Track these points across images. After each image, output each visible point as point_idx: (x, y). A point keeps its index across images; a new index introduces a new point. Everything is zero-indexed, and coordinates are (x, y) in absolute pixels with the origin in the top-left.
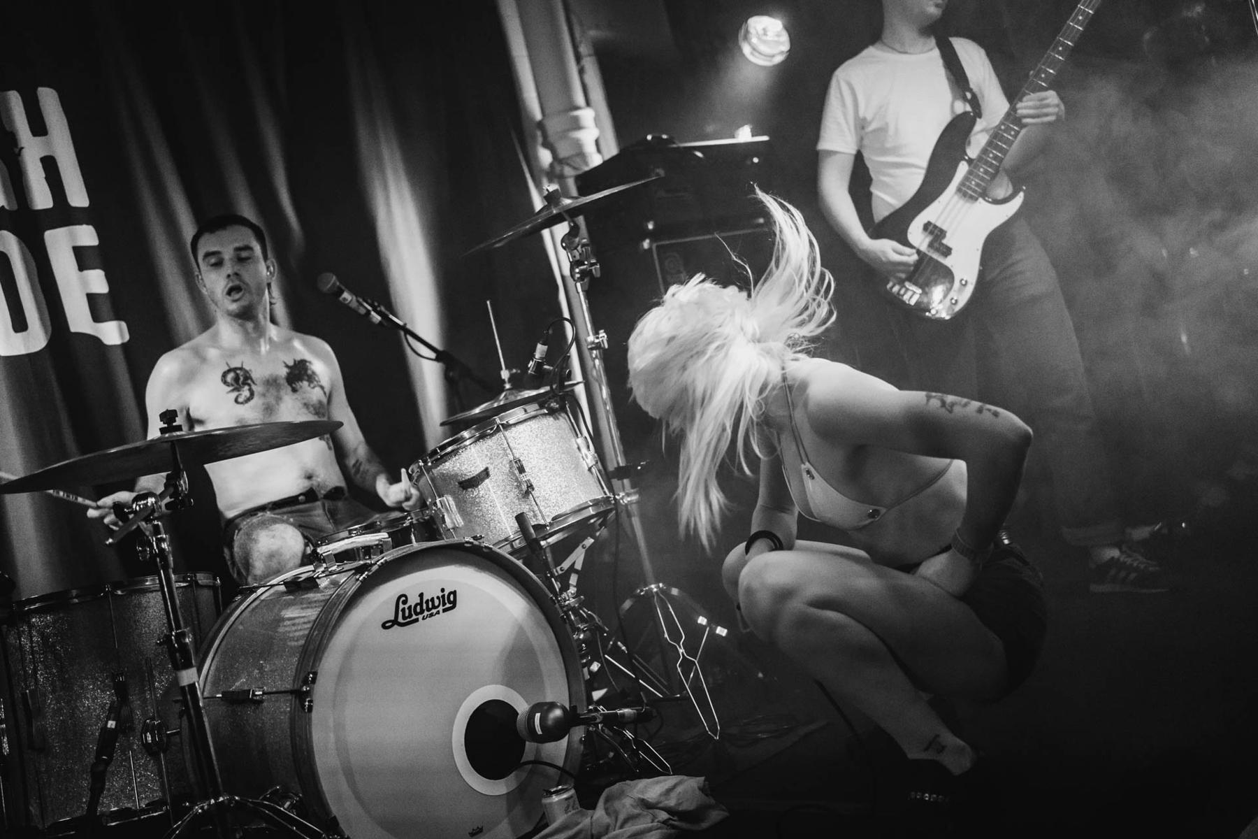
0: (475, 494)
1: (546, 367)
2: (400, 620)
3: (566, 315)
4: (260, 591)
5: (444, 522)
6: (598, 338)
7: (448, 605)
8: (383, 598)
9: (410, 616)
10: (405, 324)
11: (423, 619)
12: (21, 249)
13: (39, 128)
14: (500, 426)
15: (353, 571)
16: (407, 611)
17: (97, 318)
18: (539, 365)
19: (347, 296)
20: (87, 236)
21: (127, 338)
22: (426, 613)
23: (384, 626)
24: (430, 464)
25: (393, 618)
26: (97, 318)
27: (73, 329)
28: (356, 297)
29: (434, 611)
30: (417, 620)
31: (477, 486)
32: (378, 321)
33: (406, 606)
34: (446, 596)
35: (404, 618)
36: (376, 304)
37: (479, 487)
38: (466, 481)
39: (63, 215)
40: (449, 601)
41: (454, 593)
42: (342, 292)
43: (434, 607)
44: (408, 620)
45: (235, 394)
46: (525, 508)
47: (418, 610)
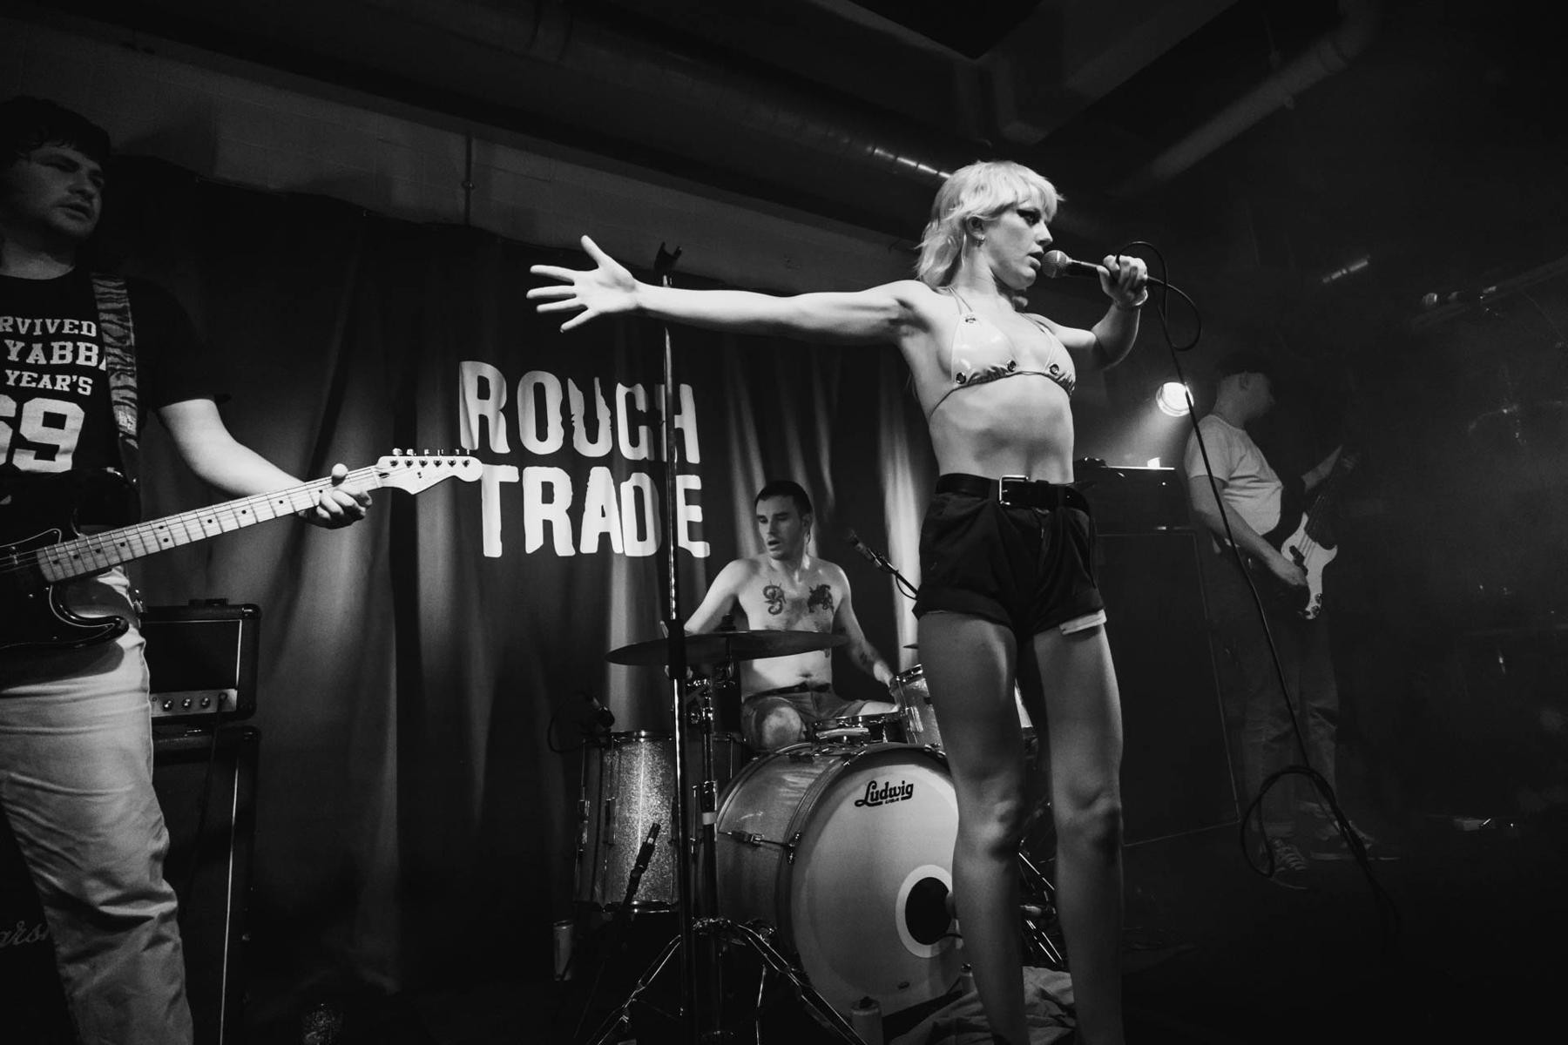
2: (869, 801)
5: (909, 726)
7: (906, 795)
8: (858, 788)
9: (877, 799)
11: (886, 803)
12: (651, 485)
13: (676, 408)
15: (839, 757)
16: (875, 795)
17: (691, 538)
22: (889, 799)
23: (857, 804)
24: (904, 681)
25: (863, 799)
26: (691, 538)
29: (895, 798)
30: (881, 803)
35: (872, 800)
40: (907, 792)
41: (912, 786)
43: (896, 795)
47: (883, 794)
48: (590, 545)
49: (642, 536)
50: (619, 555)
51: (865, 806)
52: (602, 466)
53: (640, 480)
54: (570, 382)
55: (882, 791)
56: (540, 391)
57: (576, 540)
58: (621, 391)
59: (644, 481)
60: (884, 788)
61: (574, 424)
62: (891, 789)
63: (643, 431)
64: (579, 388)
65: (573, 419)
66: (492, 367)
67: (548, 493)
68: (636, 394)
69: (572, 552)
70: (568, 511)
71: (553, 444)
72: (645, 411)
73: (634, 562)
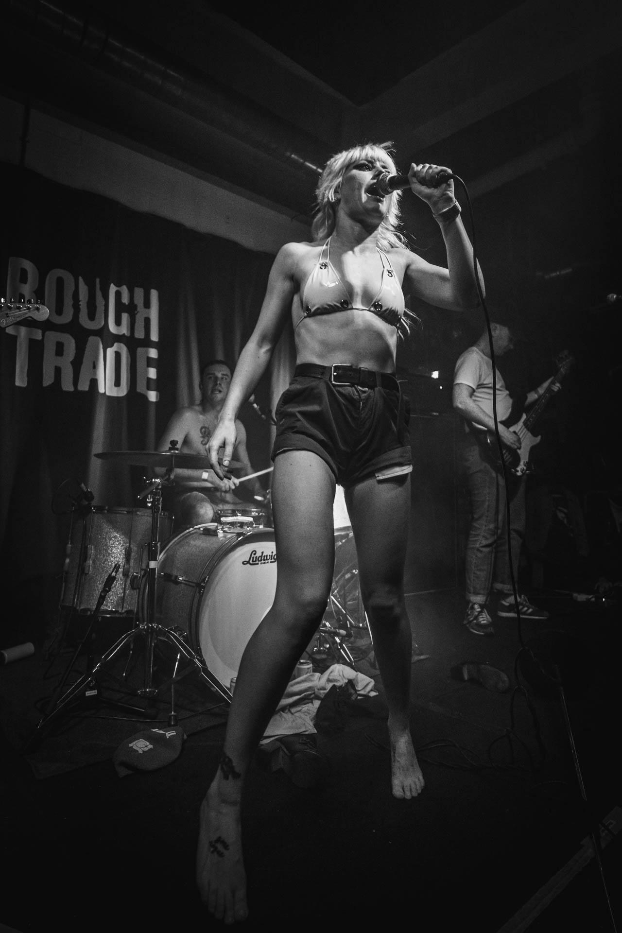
2: (251, 562)
4: (191, 529)
7: (273, 560)
9: (256, 561)
11: (261, 564)
13: (147, 305)
16: (254, 559)
22: (263, 561)
23: (243, 563)
29: (266, 561)
30: (258, 564)
33: (255, 556)
35: (253, 561)
39: (146, 342)
43: (267, 559)
44: (254, 563)
45: (202, 439)
47: (260, 559)
48: (84, 386)
49: (117, 383)
50: (103, 394)
51: (248, 565)
53: (119, 348)
54: (81, 279)
55: (259, 557)
56: (60, 282)
57: (76, 382)
58: (113, 289)
60: (261, 555)
61: (80, 307)
63: (125, 317)
64: (86, 283)
65: (80, 303)
66: (31, 263)
67: (60, 350)
68: (122, 292)
69: (71, 389)
70: (72, 363)
71: (67, 317)
72: (127, 303)
73: (112, 401)
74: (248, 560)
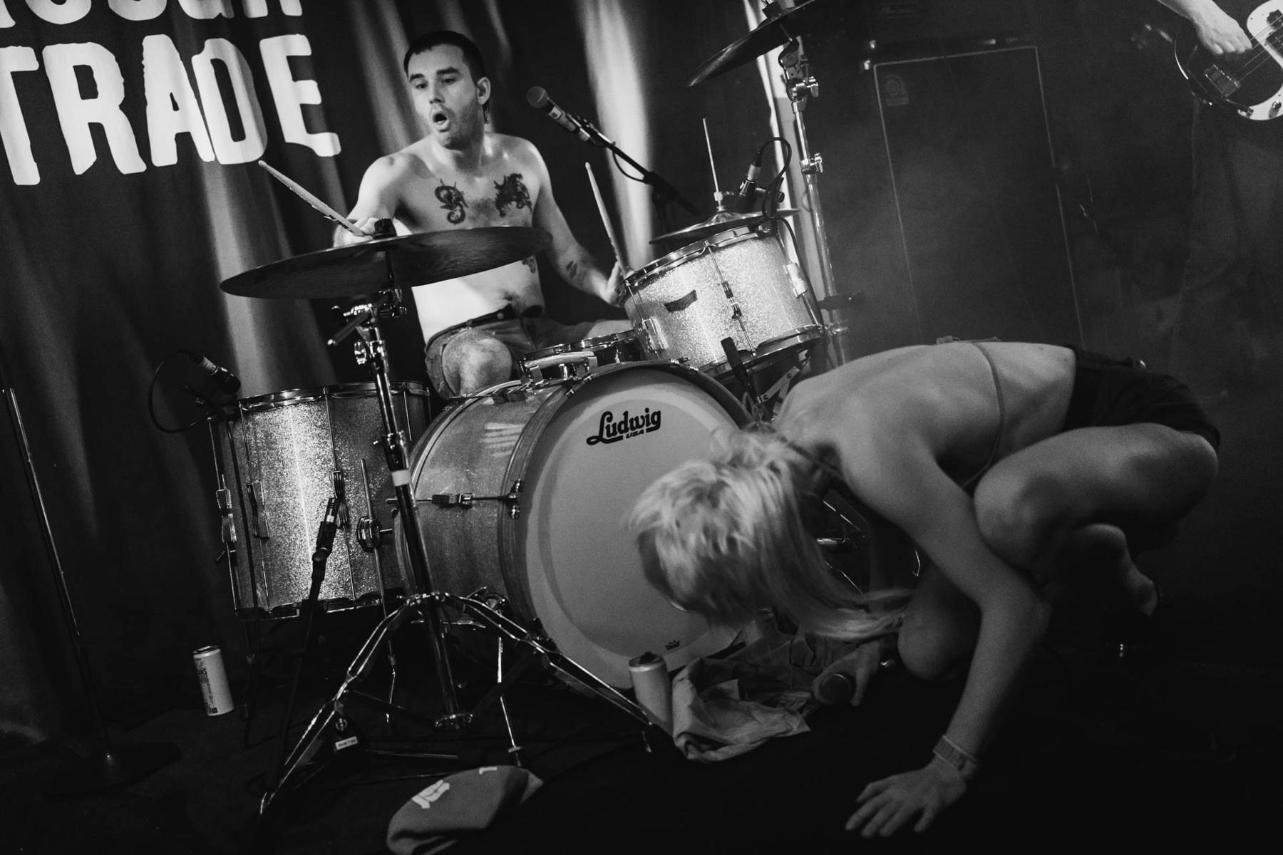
0: (681, 316)
1: (758, 189)
2: (605, 436)
3: (776, 134)
5: (649, 344)
6: (813, 161)
7: (652, 425)
8: (589, 416)
9: (615, 433)
10: (614, 143)
11: (627, 437)
14: (709, 248)
15: (559, 387)
16: (611, 431)
17: (310, 129)
18: (751, 187)
19: (556, 110)
20: (300, 45)
21: (339, 150)
22: (630, 432)
23: (589, 441)
24: (636, 284)
25: (597, 434)
27: (289, 138)
28: (566, 112)
29: (638, 430)
30: (621, 438)
31: (683, 309)
32: (587, 139)
33: (611, 424)
34: (650, 415)
35: (609, 435)
36: (585, 121)
37: (686, 310)
38: (672, 303)
39: (277, 24)
40: (653, 421)
41: (658, 414)
42: (551, 108)
43: (638, 426)
44: (612, 437)
46: (733, 333)
51: (600, 443)
52: (159, 33)
53: (219, 48)
55: (621, 423)
59: (228, 52)
60: (622, 419)
62: (632, 420)
74: (597, 434)
